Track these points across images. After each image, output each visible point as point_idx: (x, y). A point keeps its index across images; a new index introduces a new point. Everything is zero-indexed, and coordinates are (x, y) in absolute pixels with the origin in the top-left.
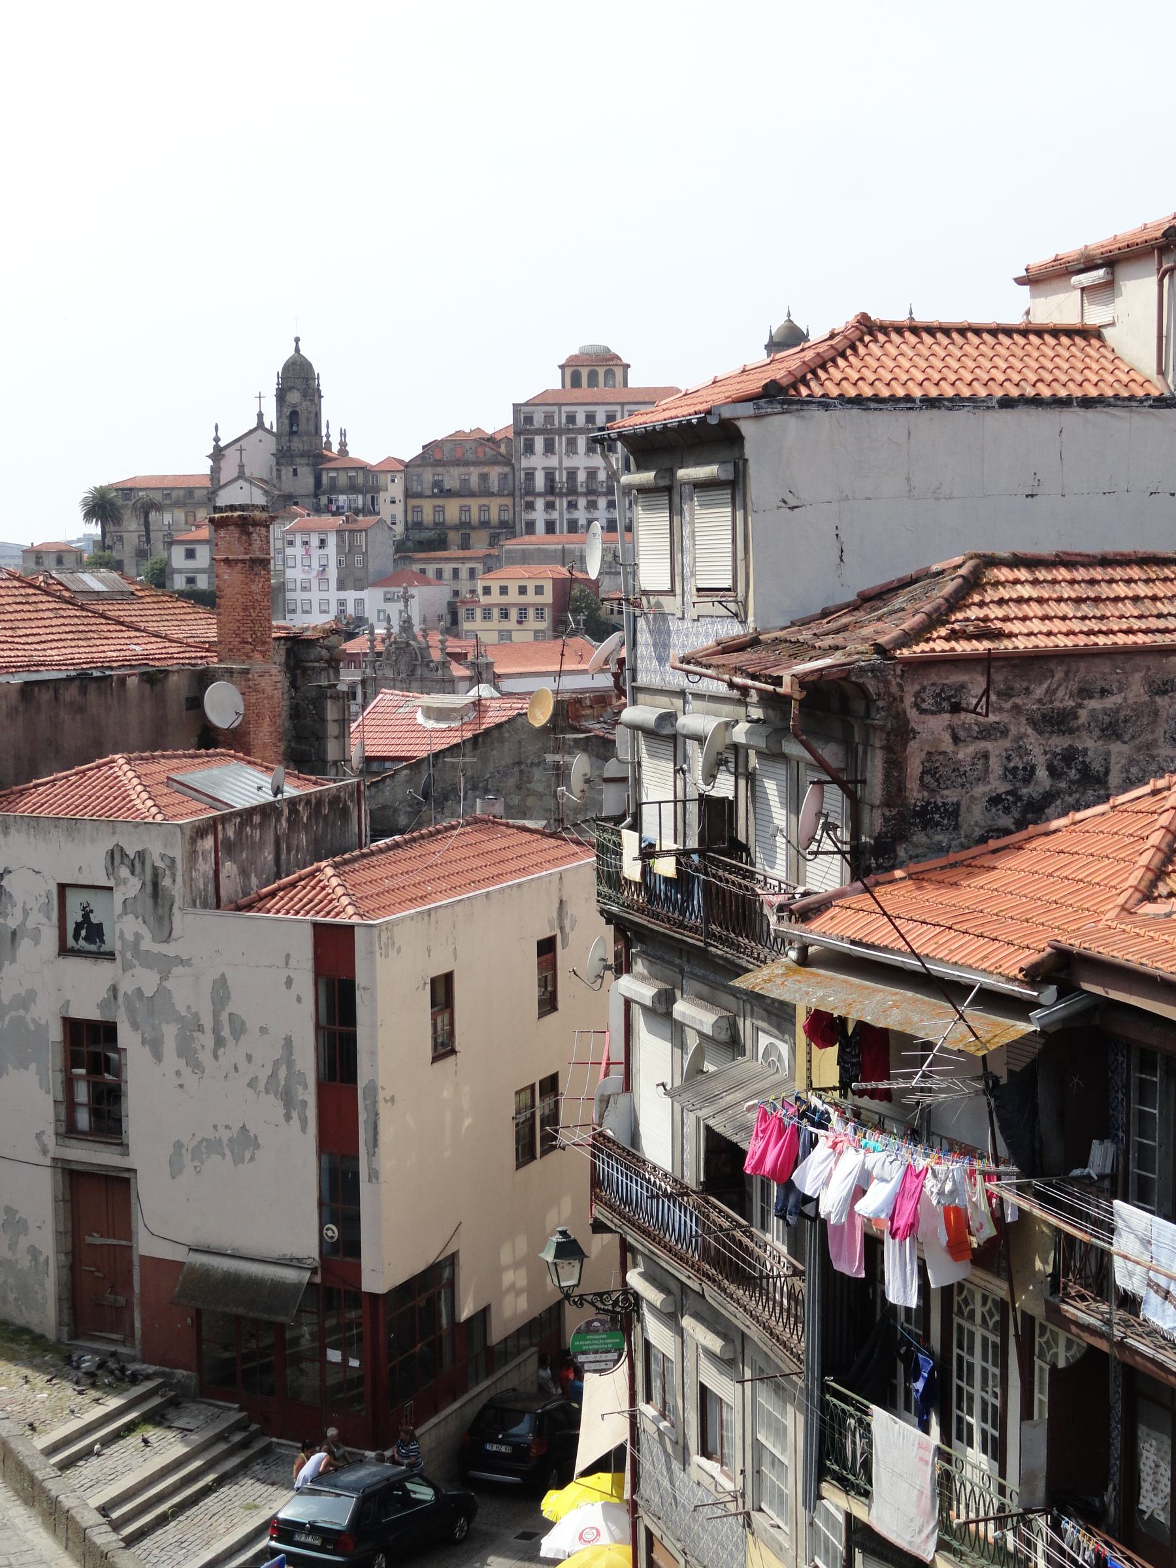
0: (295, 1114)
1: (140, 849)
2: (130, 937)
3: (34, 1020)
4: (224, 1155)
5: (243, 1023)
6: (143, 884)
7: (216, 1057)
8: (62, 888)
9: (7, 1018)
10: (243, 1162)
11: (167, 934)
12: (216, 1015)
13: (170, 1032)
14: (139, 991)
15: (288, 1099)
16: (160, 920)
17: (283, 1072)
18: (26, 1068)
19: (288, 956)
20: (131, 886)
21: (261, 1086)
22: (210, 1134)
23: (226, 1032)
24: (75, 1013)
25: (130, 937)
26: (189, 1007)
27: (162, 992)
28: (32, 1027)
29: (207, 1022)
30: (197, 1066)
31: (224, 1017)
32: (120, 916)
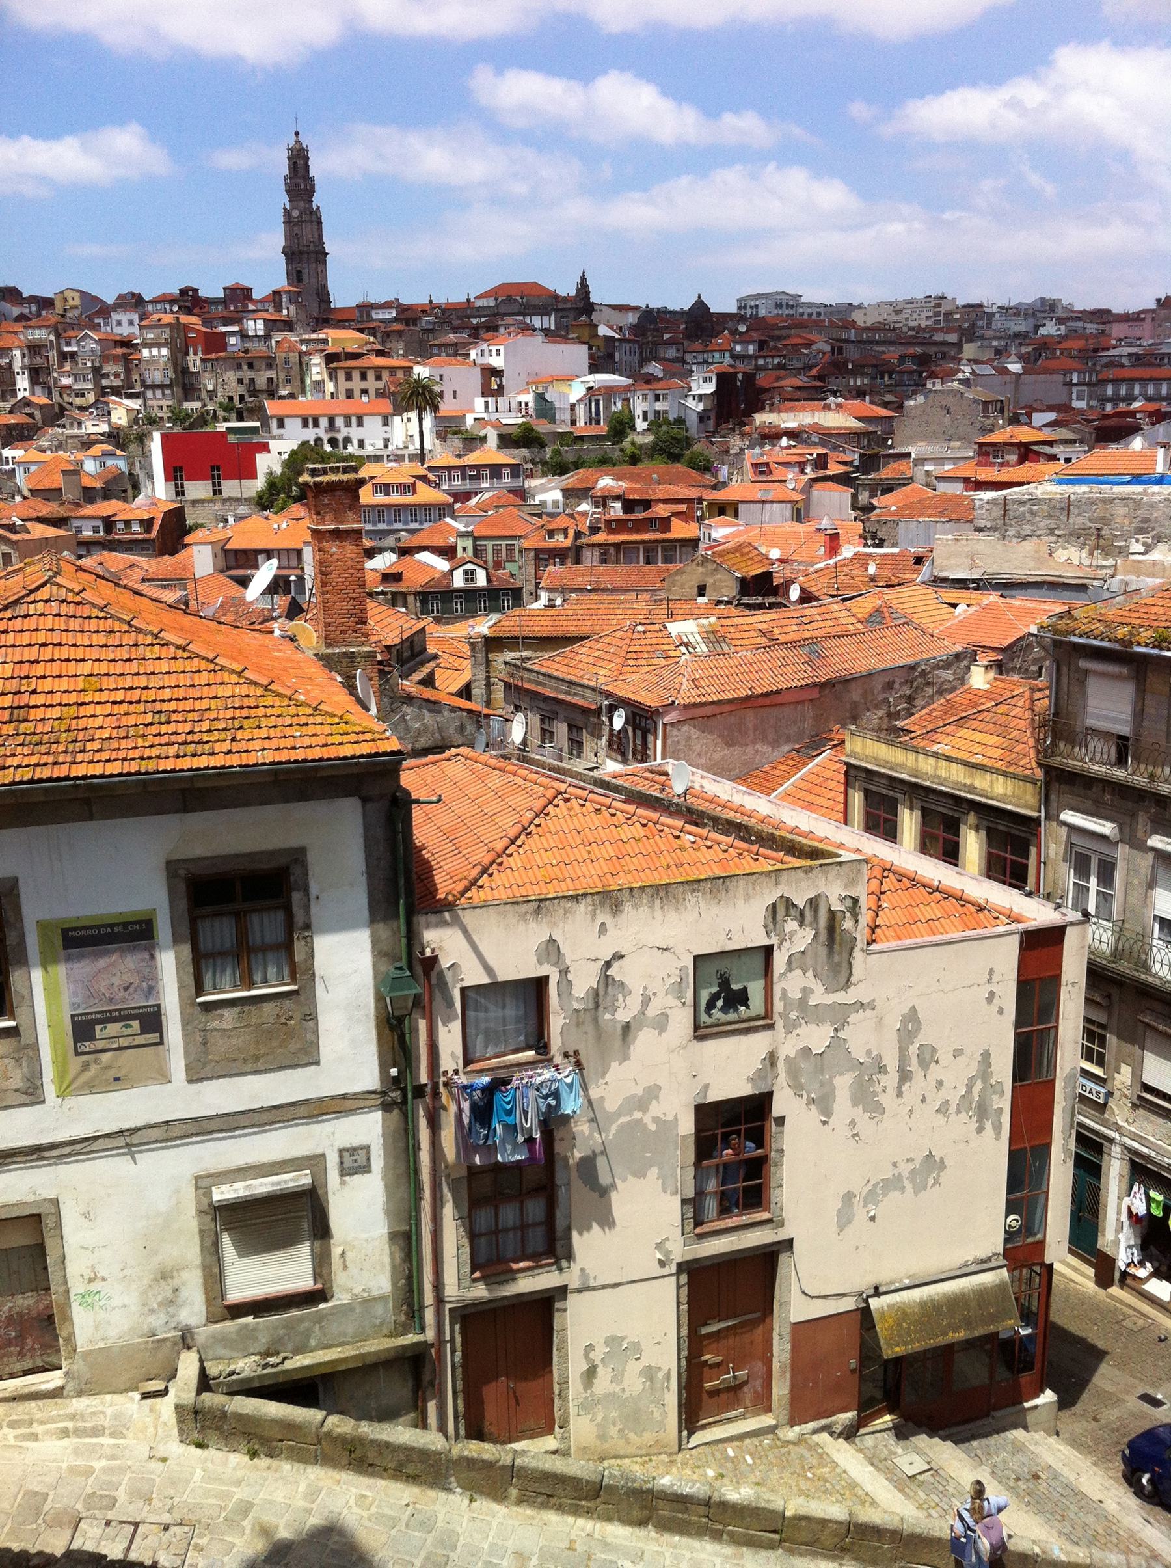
0: (988, 1125)
3: (656, 1120)
7: (900, 1094)
8: (696, 958)
9: (614, 1129)
11: (844, 980)
13: (843, 1084)
14: (807, 1050)
15: (983, 1112)
16: (835, 969)
17: (979, 1086)
18: (644, 1176)
19: (991, 971)
20: (800, 938)
23: (914, 1066)
24: (714, 1096)
26: (869, 1052)
27: (837, 1043)
28: (653, 1127)
29: (891, 1061)
30: (880, 1109)
31: (913, 1049)
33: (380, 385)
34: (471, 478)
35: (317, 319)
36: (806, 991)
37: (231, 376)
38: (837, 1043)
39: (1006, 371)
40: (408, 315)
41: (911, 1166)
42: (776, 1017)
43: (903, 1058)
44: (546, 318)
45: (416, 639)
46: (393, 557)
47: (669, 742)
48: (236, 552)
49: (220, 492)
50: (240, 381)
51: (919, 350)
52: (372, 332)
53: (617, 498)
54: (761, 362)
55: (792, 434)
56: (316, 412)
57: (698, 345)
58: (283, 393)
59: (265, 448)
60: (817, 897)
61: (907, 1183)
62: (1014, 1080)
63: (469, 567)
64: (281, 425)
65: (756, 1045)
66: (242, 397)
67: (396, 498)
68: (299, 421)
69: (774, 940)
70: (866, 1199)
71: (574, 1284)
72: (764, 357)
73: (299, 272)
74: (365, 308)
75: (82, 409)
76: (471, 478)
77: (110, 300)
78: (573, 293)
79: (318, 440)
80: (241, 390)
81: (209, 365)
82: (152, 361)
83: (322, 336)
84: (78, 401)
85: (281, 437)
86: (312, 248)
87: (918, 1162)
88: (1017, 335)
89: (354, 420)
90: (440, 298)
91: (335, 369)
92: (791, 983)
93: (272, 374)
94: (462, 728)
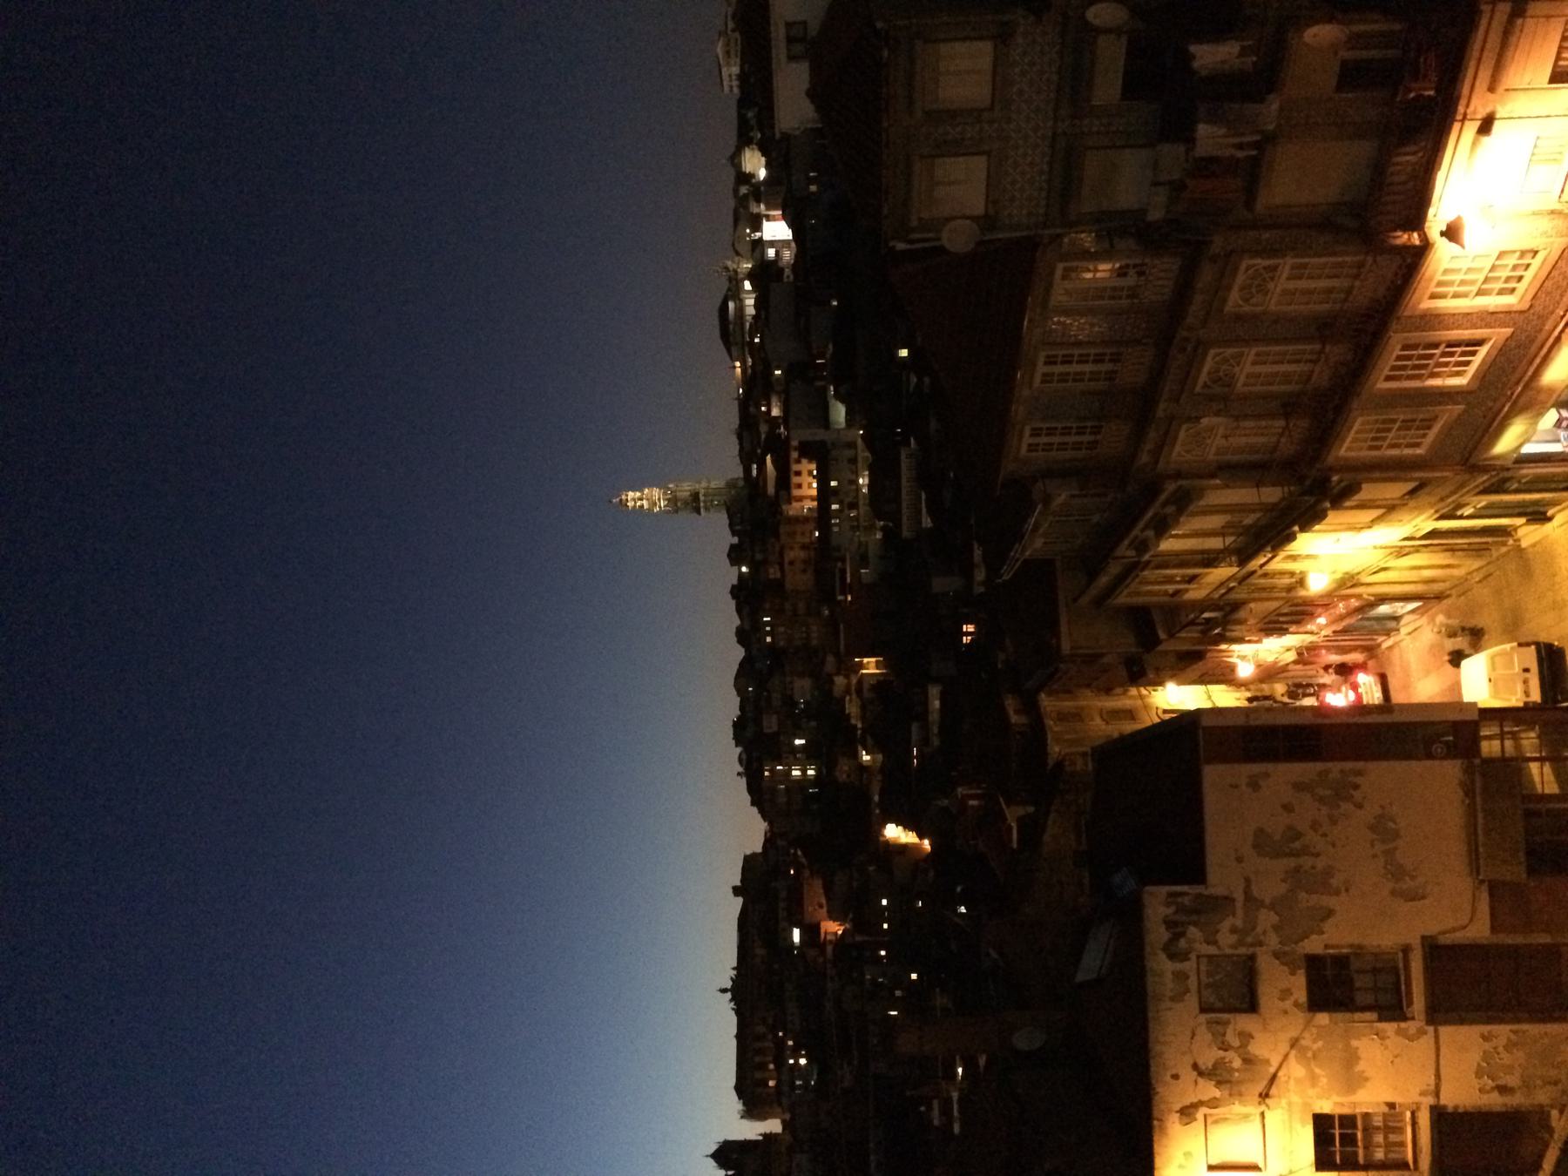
1: (1162, 929)
2: (1233, 938)
4: (1396, 848)
14: (1276, 928)
17: (1321, 792)
25: (1233, 938)
26: (1283, 881)
29: (1291, 862)
36: (1234, 930)
43: (1292, 854)
50: (804, 571)
60: (1165, 922)
61: (1391, 846)
71: (1430, 1100)
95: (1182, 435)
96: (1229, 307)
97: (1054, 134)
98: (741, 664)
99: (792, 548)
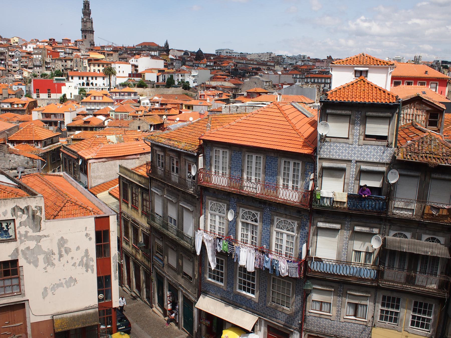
0: (89, 270)
1: (26, 206)
2: (23, 232)
4: (63, 287)
5: (70, 249)
6: (29, 216)
7: (60, 260)
10: (71, 286)
11: (39, 229)
12: (59, 249)
13: (41, 258)
14: (28, 248)
16: (36, 226)
19: (86, 228)
21: (77, 264)
22: (58, 282)
23: (64, 253)
25: (23, 232)
26: (49, 249)
29: (56, 251)
30: (53, 264)
32: (18, 227)
33: (103, 68)
34: (122, 95)
35: (89, 49)
36: (27, 232)
37: (60, 63)
38: (38, 247)
39: (277, 74)
40: (116, 50)
41: (65, 280)
42: (17, 239)
44: (156, 52)
45: (54, 139)
46: (91, 116)
47: (91, 168)
48: (45, 114)
49: (50, 97)
50: (63, 66)
51: (257, 66)
52: (104, 54)
53: (158, 103)
54: (214, 67)
55: (214, 88)
56: (83, 75)
57: (198, 62)
58: (75, 70)
59: (64, 85)
60: (28, 206)
61: (65, 285)
62: (97, 257)
63: (109, 120)
64: (72, 78)
65: (12, 246)
66: (63, 70)
67: (97, 100)
68: (78, 78)
69: (14, 218)
70: (51, 289)
72: (215, 66)
73: (85, 36)
74: (103, 47)
75: (15, 71)
76: (122, 95)
77: (29, 41)
78: (164, 46)
79: (83, 84)
80: (63, 68)
81: (54, 60)
82: (36, 59)
83: (88, 54)
84: (14, 69)
85: (71, 82)
86: (89, 29)
87: (67, 279)
88: (291, 64)
89: (94, 79)
90: (126, 45)
91: (90, 63)
92: (22, 230)
93: (72, 64)
94: (27, 163)
95: (221, 204)
96: (276, 218)
97: (350, 161)
98: (24, 40)
99: (71, 61)
